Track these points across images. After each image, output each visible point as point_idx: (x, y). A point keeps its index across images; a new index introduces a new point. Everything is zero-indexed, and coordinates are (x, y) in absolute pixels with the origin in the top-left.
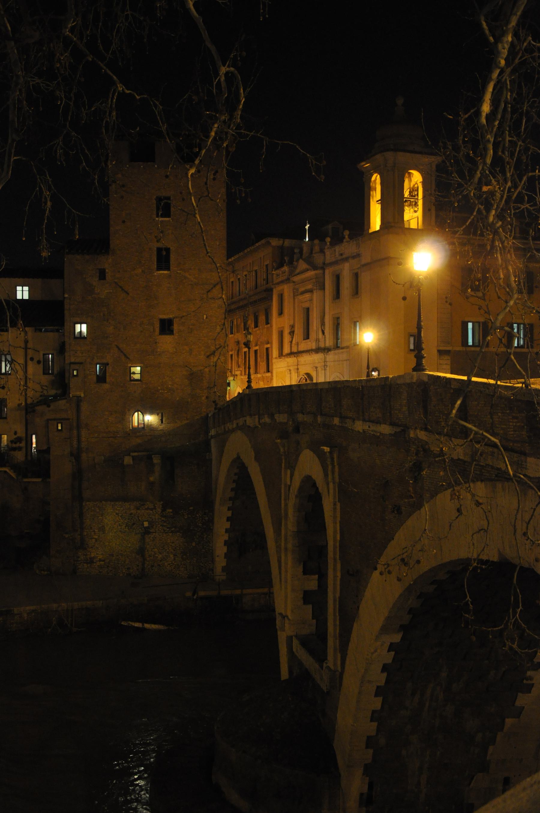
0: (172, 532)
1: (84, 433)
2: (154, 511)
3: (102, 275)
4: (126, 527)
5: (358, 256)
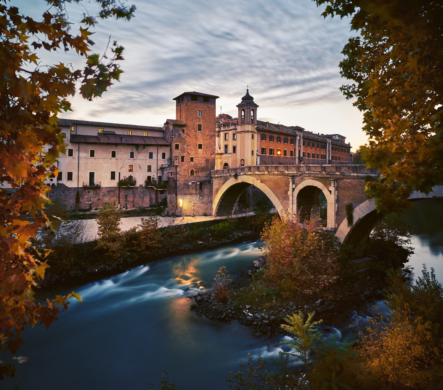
1: (178, 175)
3: (183, 131)
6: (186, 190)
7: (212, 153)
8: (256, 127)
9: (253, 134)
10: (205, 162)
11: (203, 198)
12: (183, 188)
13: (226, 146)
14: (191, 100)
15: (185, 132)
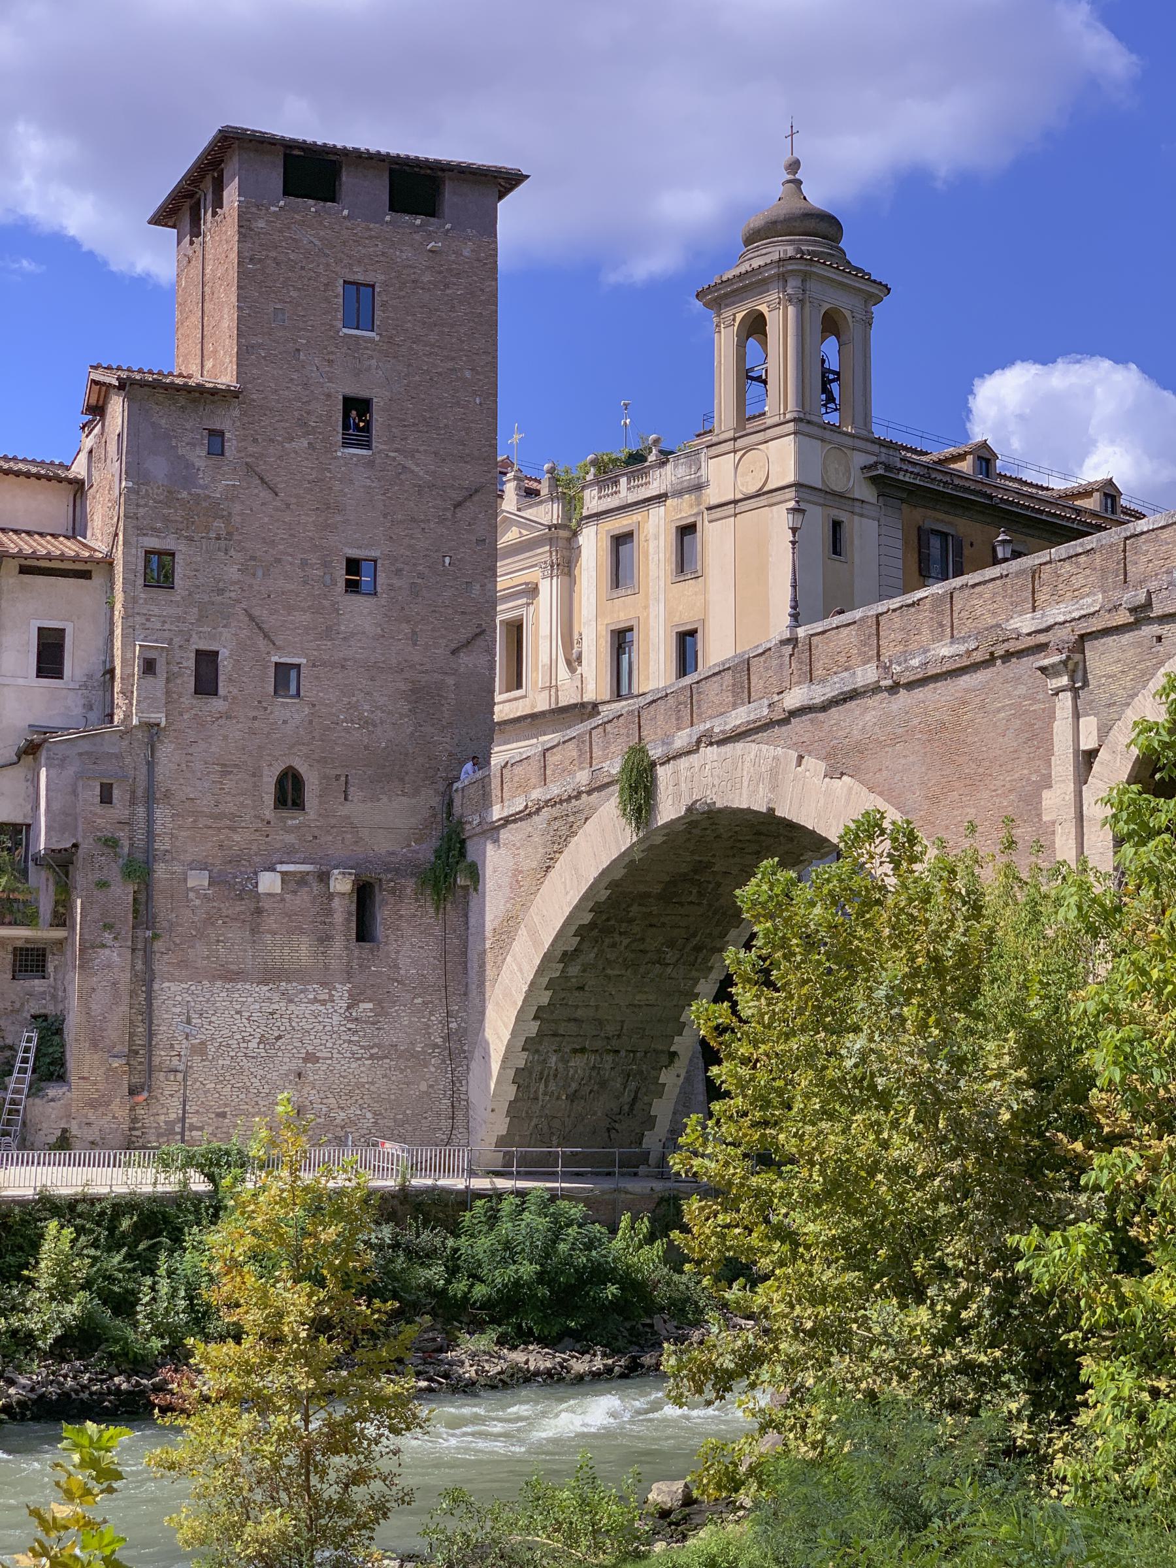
0: (372, 1057)
1: (162, 814)
2: (329, 1005)
4: (259, 1043)
5: (698, 488)
6: (236, 934)
7: (465, 634)
8: (861, 459)
9: (843, 516)
10: (404, 706)
11: (381, 1011)
12: (209, 921)
13: (621, 640)
14: (287, 192)
15: (231, 448)
